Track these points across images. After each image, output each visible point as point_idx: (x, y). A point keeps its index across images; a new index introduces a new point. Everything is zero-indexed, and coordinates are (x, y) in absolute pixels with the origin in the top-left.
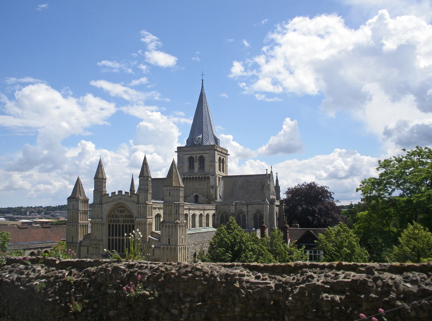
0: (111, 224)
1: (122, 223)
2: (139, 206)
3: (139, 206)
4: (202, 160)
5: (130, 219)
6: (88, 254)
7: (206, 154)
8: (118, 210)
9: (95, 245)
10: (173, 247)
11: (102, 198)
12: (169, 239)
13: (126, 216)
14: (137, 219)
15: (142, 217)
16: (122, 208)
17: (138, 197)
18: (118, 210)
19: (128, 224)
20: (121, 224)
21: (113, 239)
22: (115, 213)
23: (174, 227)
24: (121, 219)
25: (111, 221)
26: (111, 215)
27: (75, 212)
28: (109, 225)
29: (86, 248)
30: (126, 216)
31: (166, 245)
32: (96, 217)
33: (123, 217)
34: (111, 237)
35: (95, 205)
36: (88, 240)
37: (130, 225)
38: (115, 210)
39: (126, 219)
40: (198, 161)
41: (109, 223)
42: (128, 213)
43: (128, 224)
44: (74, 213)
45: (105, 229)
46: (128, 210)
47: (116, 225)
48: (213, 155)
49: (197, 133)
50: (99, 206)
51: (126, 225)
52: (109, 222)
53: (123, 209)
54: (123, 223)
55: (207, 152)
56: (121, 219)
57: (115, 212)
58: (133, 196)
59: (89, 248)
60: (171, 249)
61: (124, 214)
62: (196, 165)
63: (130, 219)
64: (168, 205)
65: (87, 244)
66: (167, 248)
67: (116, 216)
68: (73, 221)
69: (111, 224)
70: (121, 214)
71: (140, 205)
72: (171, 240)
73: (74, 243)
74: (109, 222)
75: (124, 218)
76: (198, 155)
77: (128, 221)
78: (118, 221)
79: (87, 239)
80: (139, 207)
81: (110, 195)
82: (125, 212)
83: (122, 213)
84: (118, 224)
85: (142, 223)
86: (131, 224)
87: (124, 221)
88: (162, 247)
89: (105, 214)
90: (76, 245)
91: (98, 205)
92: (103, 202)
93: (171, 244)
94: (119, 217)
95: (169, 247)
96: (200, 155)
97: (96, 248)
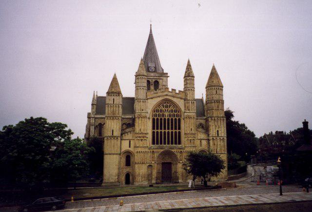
0: (156, 118)
4: (156, 84)
5: (176, 114)
6: (130, 147)
10: (221, 138)
12: (218, 131)
13: (172, 111)
14: (185, 114)
19: (174, 118)
21: (157, 132)
25: (156, 115)
26: (155, 110)
28: (154, 120)
29: (128, 141)
34: (156, 131)
37: (176, 119)
39: (172, 114)
43: (174, 118)
45: (150, 124)
47: (161, 119)
51: (172, 119)
53: (168, 105)
55: (161, 78)
56: (166, 114)
59: (131, 143)
62: (152, 87)
63: (176, 114)
65: (129, 138)
67: (161, 111)
69: (156, 118)
77: (174, 115)
78: (163, 115)
84: (163, 118)
86: (177, 118)
87: (170, 115)
93: (220, 135)
95: (218, 138)
97: (142, 140)
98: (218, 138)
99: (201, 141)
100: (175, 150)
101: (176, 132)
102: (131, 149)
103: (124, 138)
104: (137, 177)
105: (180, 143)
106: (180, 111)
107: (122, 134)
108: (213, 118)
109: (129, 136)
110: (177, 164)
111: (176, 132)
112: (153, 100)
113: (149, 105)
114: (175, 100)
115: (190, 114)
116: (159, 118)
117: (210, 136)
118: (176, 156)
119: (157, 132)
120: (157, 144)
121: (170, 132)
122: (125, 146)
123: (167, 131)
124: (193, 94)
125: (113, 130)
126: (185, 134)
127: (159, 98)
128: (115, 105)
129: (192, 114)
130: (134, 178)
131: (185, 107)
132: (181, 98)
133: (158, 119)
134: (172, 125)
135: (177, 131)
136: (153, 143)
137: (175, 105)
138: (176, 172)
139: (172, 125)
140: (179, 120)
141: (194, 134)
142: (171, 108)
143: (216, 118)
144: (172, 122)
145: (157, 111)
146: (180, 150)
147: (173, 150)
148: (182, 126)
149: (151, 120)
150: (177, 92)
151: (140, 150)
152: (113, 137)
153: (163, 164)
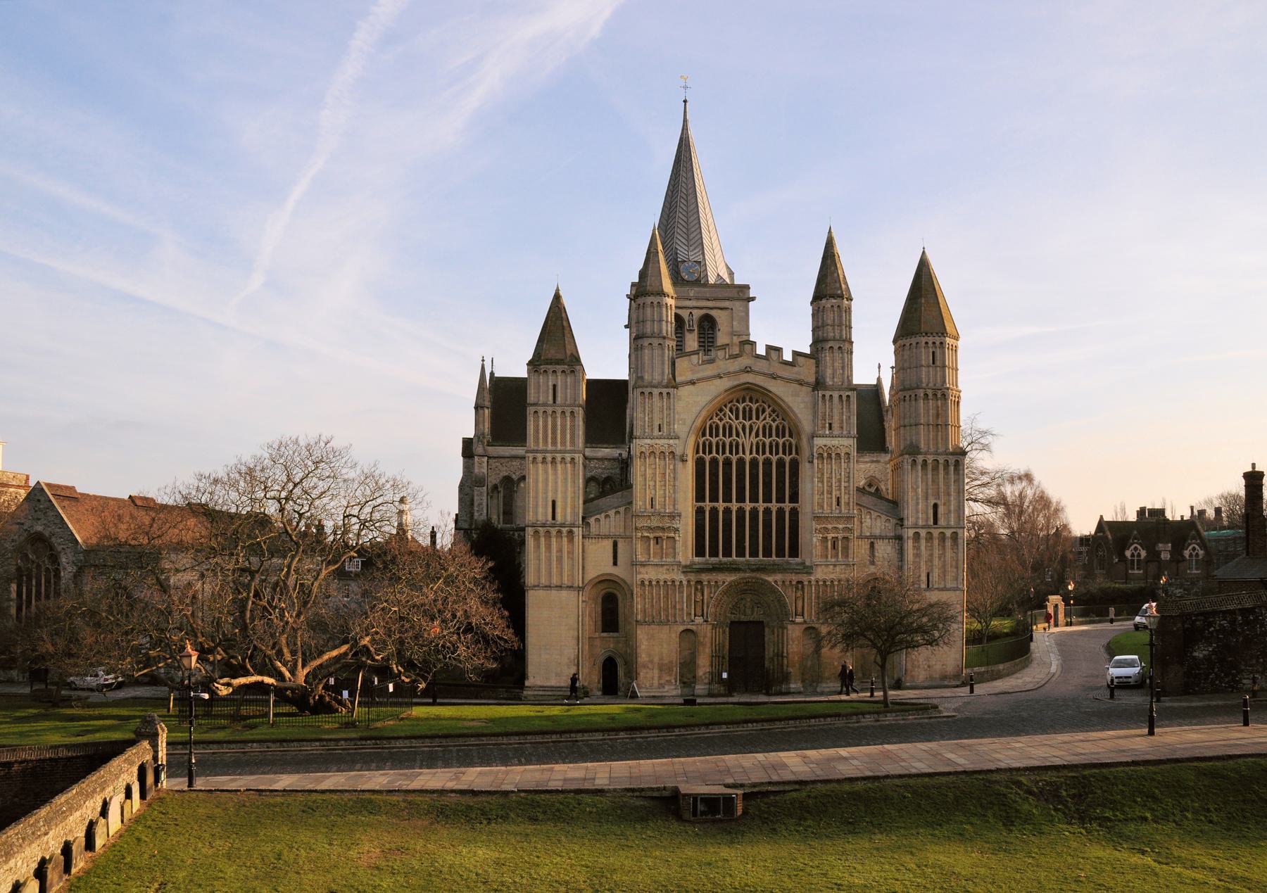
0: (707, 458)
1: (751, 453)
2: (824, 396)
3: (824, 396)
4: (708, 325)
5: (781, 441)
6: (615, 563)
7: (720, 311)
8: (734, 408)
9: (650, 529)
10: (948, 533)
11: (673, 364)
12: (936, 506)
13: (767, 431)
14: (819, 442)
15: (836, 431)
16: (751, 400)
17: (817, 367)
18: (734, 408)
19: (774, 459)
20: (748, 458)
21: (714, 512)
22: (721, 420)
23: (952, 468)
24: (747, 441)
25: (707, 448)
27: (563, 412)
28: (700, 464)
29: (608, 544)
30: (767, 431)
31: (922, 527)
32: (656, 432)
33: (753, 433)
34: (707, 505)
35: (649, 390)
36: (618, 512)
37: (781, 463)
38: (721, 410)
39: (767, 441)
40: (696, 328)
41: (701, 454)
42: (774, 420)
43: (774, 459)
44: (559, 415)
46: (774, 411)
47: (727, 463)
48: (743, 314)
49: (686, 248)
50: (665, 391)
51: (767, 463)
52: (698, 452)
53: (754, 407)
54: (754, 454)
55: (727, 304)
56: (747, 441)
57: (724, 415)
58: (801, 360)
59: (620, 546)
60: (943, 537)
61: (760, 424)
62: (692, 342)
63: (781, 441)
64: (930, 393)
66: (930, 537)
67: (728, 430)
68: (554, 443)
69: (707, 458)
70: (747, 424)
71: (830, 393)
72: (941, 510)
73: (563, 525)
74: (698, 452)
75: (757, 435)
76: (697, 314)
77: (774, 448)
78: (735, 447)
79: (612, 513)
80: (827, 398)
81: (761, 350)
82: (762, 418)
83: (750, 419)
84: (734, 458)
85: (838, 455)
86: (787, 459)
87: (760, 448)
88: (911, 532)
89: (689, 422)
90: (571, 532)
91: (660, 390)
92: (678, 379)
93: (942, 522)
94: (738, 435)
96: (704, 312)
98: (936, 533)
99: (872, 545)
100: (779, 577)
101: (781, 512)
102: (619, 572)
103: (594, 529)
104: (642, 673)
105: (794, 552)
106: (794, 431)
107: (583, 518)
108: (920, 459)
109: (610, 523)
110: (783, 628)
111: (781, 512)
112: (700, 386)
113: (679, 406)
114: (776, 388)
115: (835, 442)
116: (721, 458)
117: (909, 521)
118: (780, 599)
119: (714, 512)
120: (714, 553)
121: (761, 510)
122: (599, 560)
123: (748, 506)
124: (847, 366)
125: (554, 503)
126: (817, 518)
127: (717, 382)
128: (559, 410)
129: (846, 442)
130: (632, 674)
131: (815, 413)
132: (801, 383)
133: (714, 462)
134: (767, 485)
135: (787, 506)
136: (699, 551)
137: (779, 410)
138: (780, 655)
139: (767, 485)
140: (795, 465)
141: (849, 518)
142: (766, 420)
143: (930, 459)
144: (767, 475)
145: (714, 430)
146: (795, 578)
147: (770, 579)
148: (809, 486)
149: (690, 466)
150: (788, 356)
151: (650, 574)
152: (553, 527)
153: (734, 625)
